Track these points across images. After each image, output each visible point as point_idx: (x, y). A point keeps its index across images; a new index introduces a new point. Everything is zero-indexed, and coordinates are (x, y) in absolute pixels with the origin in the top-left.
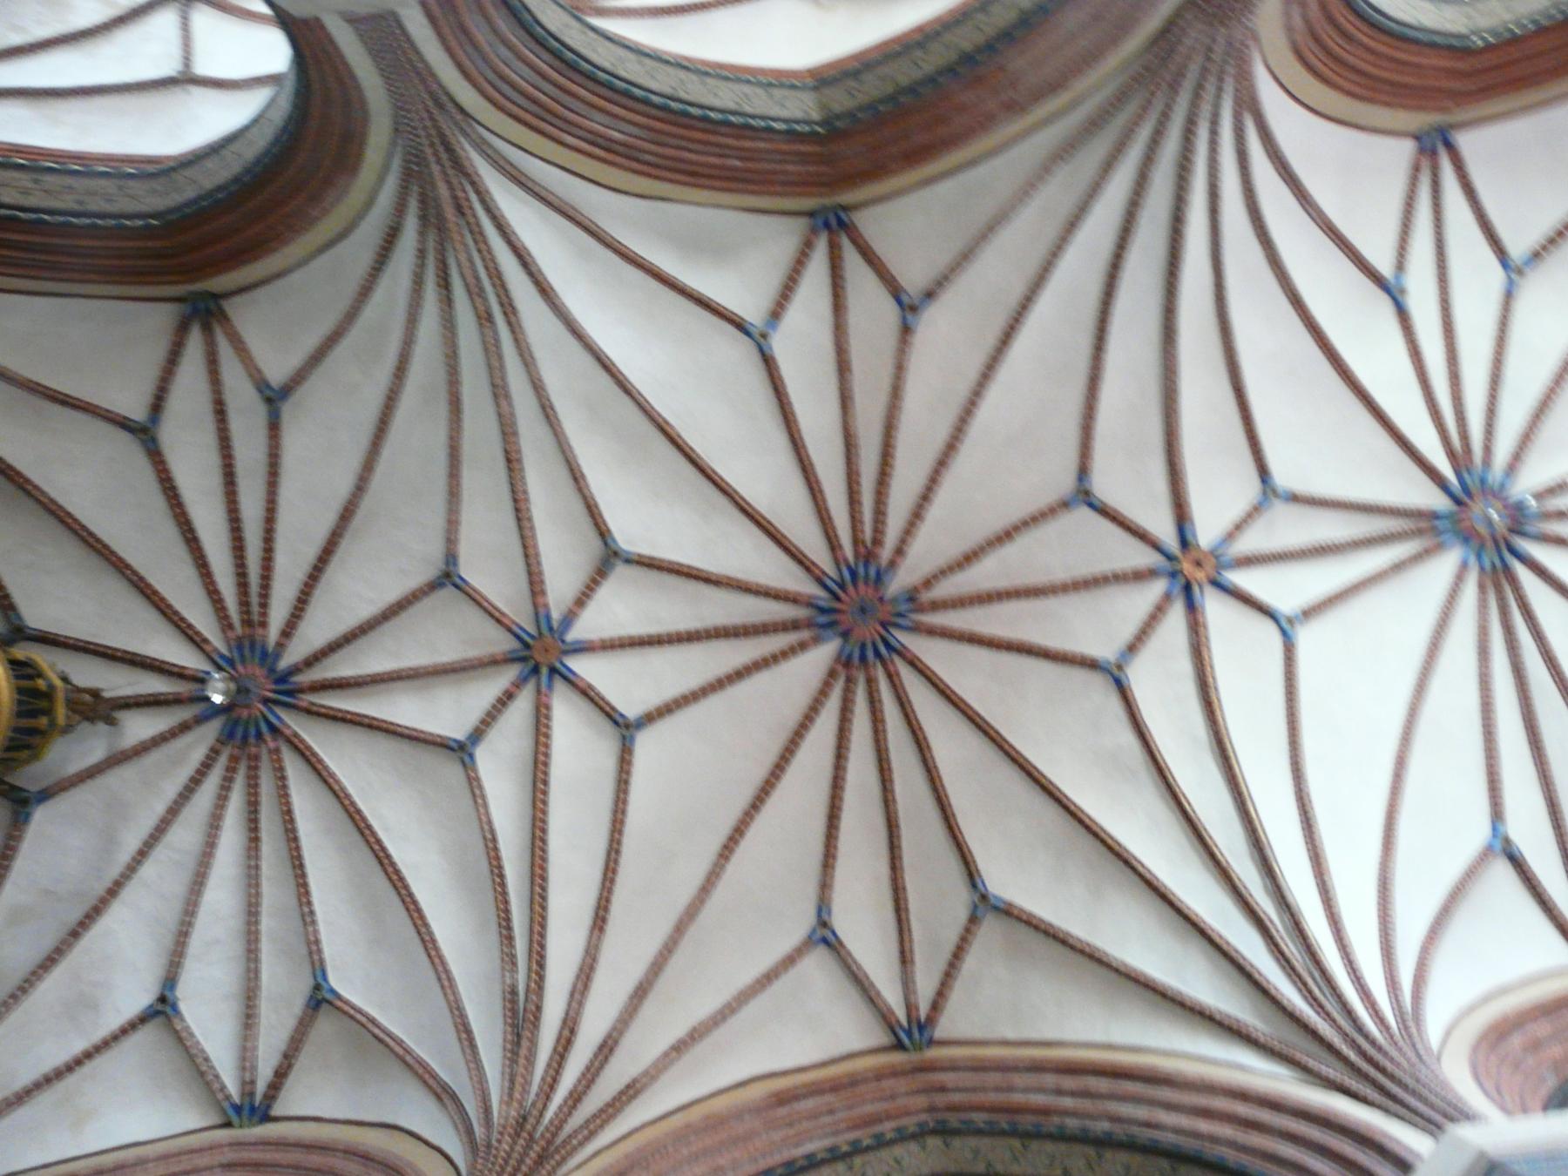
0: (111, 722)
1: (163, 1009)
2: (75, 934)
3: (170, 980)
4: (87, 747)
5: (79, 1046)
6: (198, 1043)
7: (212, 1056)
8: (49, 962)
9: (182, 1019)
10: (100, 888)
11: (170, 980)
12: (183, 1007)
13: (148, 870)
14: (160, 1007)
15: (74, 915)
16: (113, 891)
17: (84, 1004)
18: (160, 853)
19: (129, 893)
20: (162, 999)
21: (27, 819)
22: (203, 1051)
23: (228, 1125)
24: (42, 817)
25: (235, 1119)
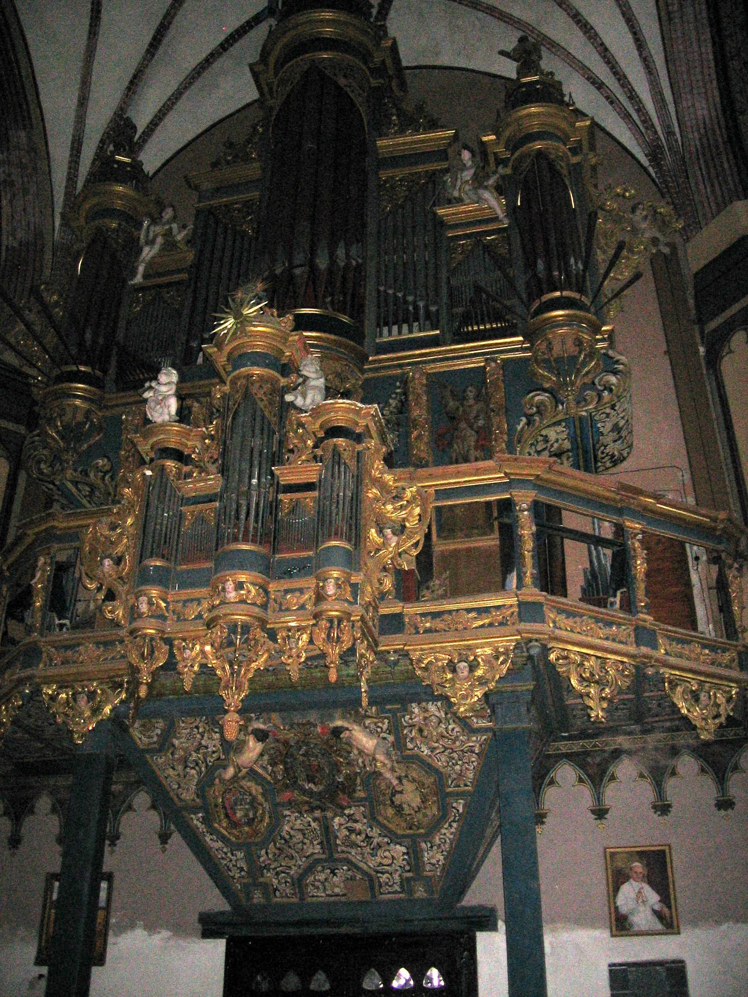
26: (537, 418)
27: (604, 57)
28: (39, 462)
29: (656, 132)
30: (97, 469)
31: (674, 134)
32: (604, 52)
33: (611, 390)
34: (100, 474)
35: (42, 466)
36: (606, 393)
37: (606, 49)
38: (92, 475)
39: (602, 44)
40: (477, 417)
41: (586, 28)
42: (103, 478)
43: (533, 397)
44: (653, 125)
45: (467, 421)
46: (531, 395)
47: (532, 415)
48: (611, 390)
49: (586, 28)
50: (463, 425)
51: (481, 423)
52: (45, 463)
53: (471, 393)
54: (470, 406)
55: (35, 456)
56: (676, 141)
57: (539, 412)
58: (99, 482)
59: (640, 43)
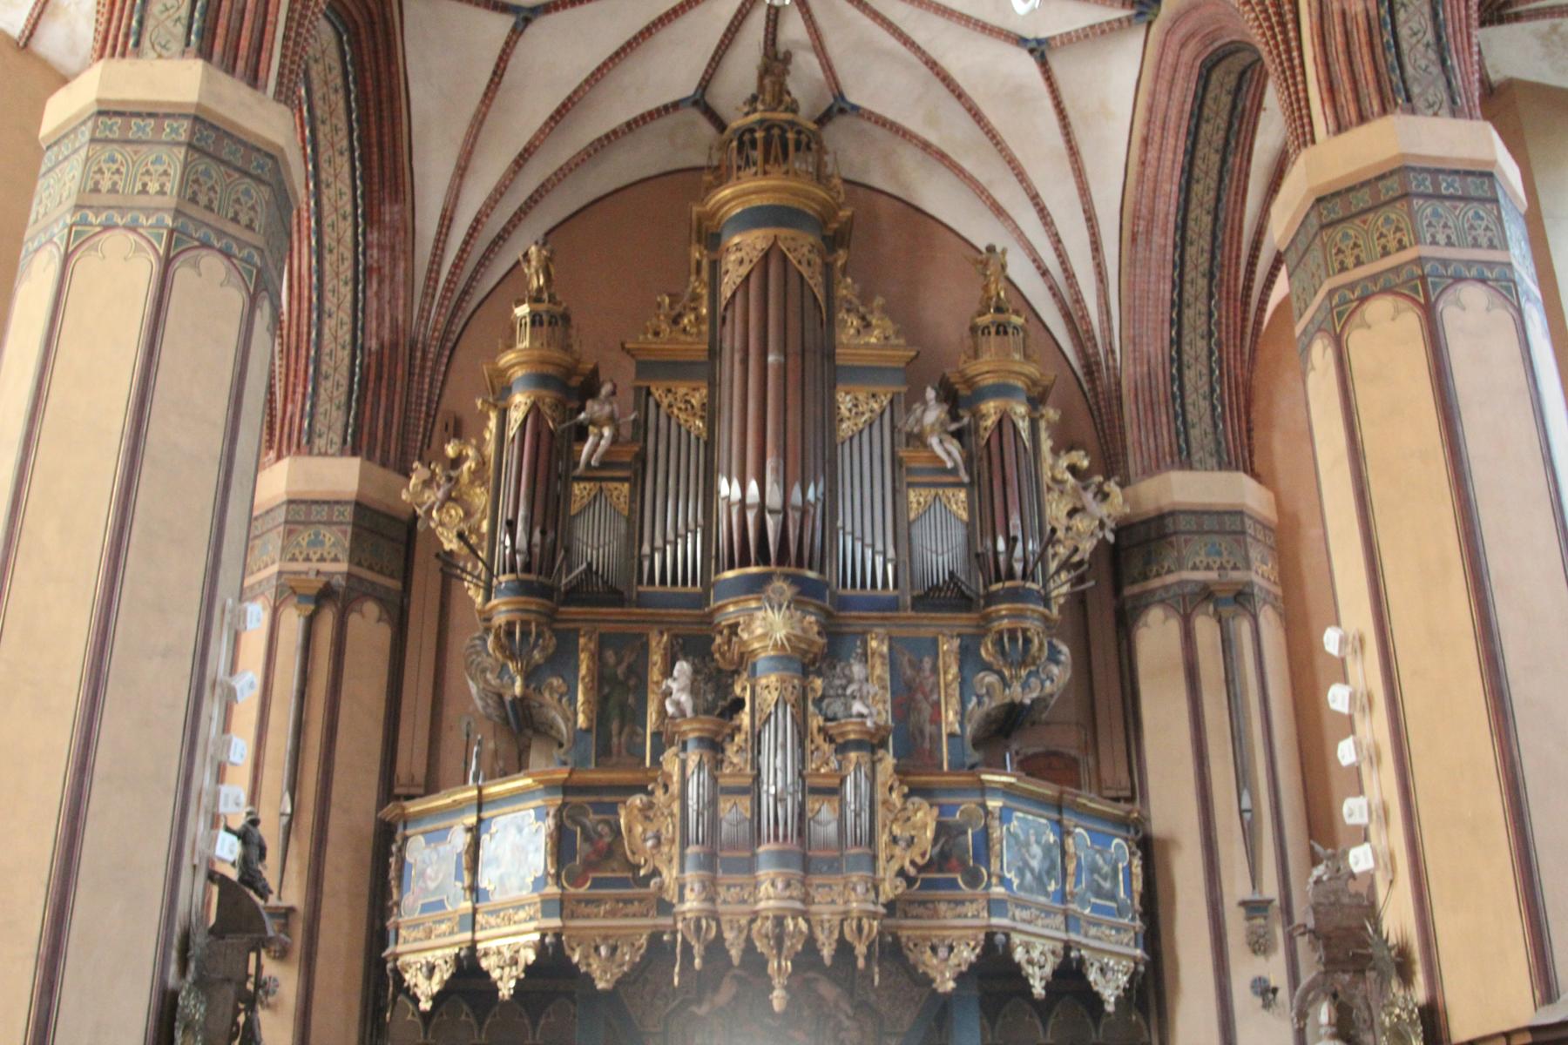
0: (788, 57)
1: (1040, 50)
2: (959, 94)
3: (1021, 41)
4: (805, 77)
5: (1048, 103)
6: (1076, 31)
7: (1091, 22)
8: (976, 115)
9: (1054, 38)
10: (924, 70)
11: (1021, 41)
12: (1043, 35)
13: (919, 37)
14: (1038, 54)
15: (940, 89)
16: (932, 65)
17: (1016, 95)
18: (907, 28)
19: (933, 53)
20: (1032, 51)
21: (855, 108)
22: (1084, 29)
23: (1150, 24)
24: (853, 98)
25: (1148, 17)
26: (986, 699)
27: (1056, 249)
28: (484, 671)
29: (1095, 345)
30: (552, 689)
31: (1113, 352)
32: (1057, 242)
33: (1052, 681)
34: (556, 696)
35: (489, 676)
36: (1048, 683)
37: (1059, 241)
38: (547, 695)
39: (1057, 234)
40: (932, 691)
41: (1043, 212)
42: (560, 700)
43: (983, 678)
44: (1094, 337)
45: (924, 693)
46: (982, 674)
47: (982, 696)
48: (1052, 681)
49: (1043, 212)
50: (919, 696)
51: (935, 697)
52: (492, 672)
53: (927, 663)
54: (926, 678)
55: (479, 664)
56: (1115, 360)
57: (988, 693)
58: (555, 703)
59: (1096, 247)
